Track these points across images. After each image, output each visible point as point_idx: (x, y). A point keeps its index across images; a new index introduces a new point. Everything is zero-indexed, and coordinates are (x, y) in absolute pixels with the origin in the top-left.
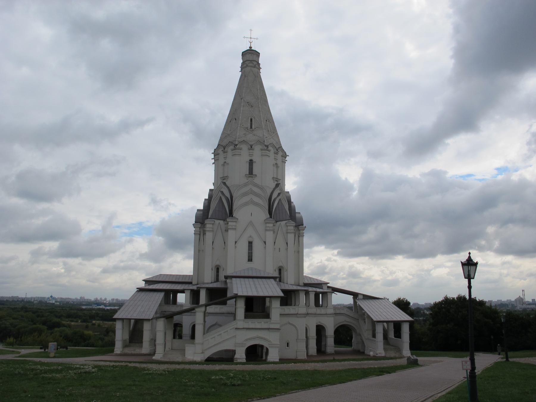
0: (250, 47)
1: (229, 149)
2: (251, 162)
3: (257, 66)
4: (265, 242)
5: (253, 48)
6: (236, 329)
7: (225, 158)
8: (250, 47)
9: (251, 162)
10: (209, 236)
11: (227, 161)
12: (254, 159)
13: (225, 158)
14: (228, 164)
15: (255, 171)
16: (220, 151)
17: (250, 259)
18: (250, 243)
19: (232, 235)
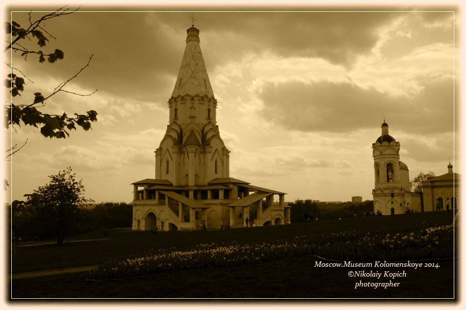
0: (193, 26)
1: (196, 99)
2: (209, 110)
3: (197, 40)
4: (223, 163)
5: (195, 27)
6: (272, 210)
7: (192, 104)
8: (193, 26)
9: (209, 110)
10: (191, 155)
11: (194, 106)
12: (210, 107)
13: (192, 104)
14: (194, 108)
15: (211, 117)
16: (188, 98)
17: (216, 173)
18: (216, 162)
19: (209, 156)
